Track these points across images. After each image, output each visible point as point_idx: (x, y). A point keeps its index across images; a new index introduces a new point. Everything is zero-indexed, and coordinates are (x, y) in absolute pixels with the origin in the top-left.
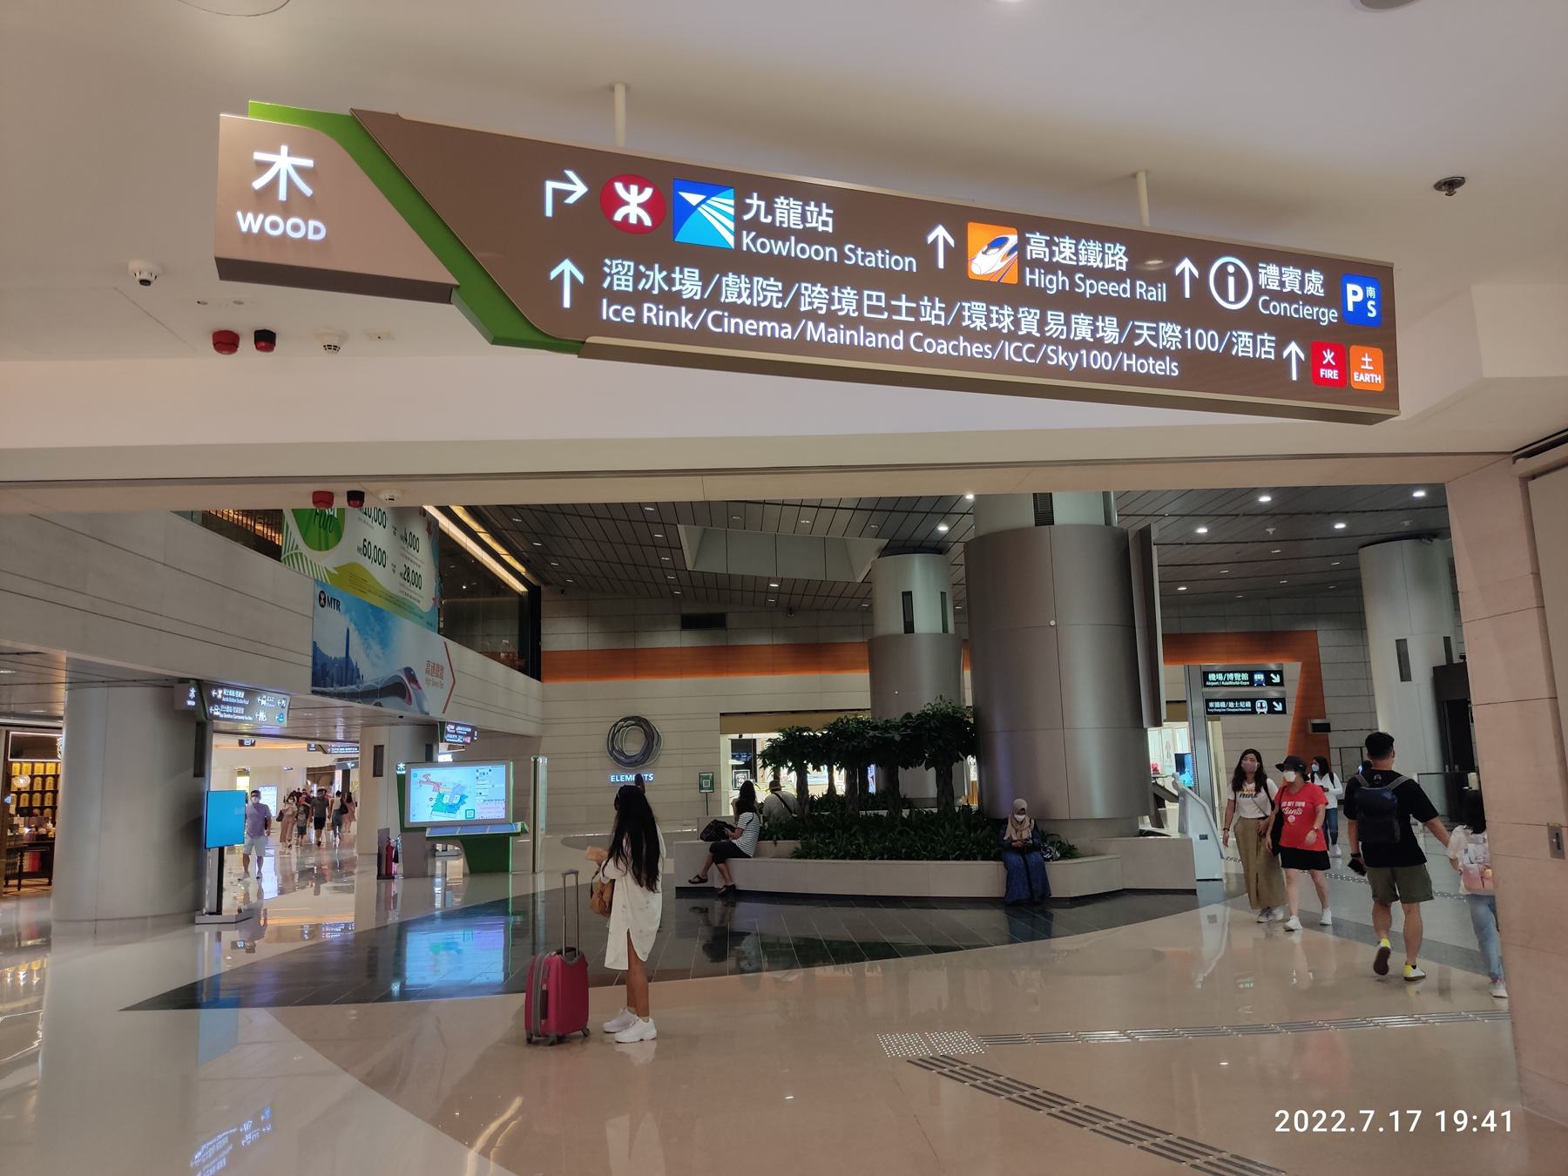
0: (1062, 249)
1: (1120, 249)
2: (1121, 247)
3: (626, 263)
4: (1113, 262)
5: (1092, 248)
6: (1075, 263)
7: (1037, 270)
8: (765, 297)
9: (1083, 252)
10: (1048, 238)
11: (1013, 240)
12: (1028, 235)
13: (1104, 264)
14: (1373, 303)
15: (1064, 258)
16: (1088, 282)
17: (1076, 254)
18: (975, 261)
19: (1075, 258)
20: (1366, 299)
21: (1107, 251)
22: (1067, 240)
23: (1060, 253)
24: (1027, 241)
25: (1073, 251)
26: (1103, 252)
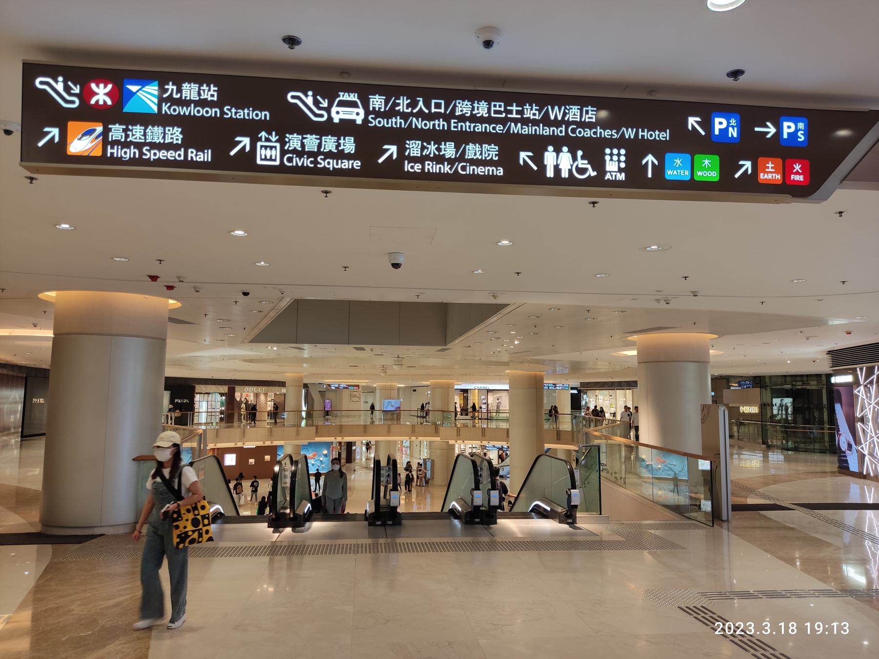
0: (134, 133)
1: (177, 131)
2: (178, 129)
3: (417, 142)
4: (171, 138)
5: (156, 131)
6: (143, 141)
7: (116, 147)
8: (489, 154)
9: (149, 134)
10: (124, 127)
11: (99, 129)
12: (110, 126)
13: (165, 140)
14: (802, 132)
15: (136, 138)
16: (152, 152)
17: (145, 135)
18: (72, 144)
19: (143, 138)
20: (797, 130)
21: (167, 132)
22: (138, 127)
23: (133, 135)
24: (110, 130)
25: (142, 133)
26: (165, 133)
